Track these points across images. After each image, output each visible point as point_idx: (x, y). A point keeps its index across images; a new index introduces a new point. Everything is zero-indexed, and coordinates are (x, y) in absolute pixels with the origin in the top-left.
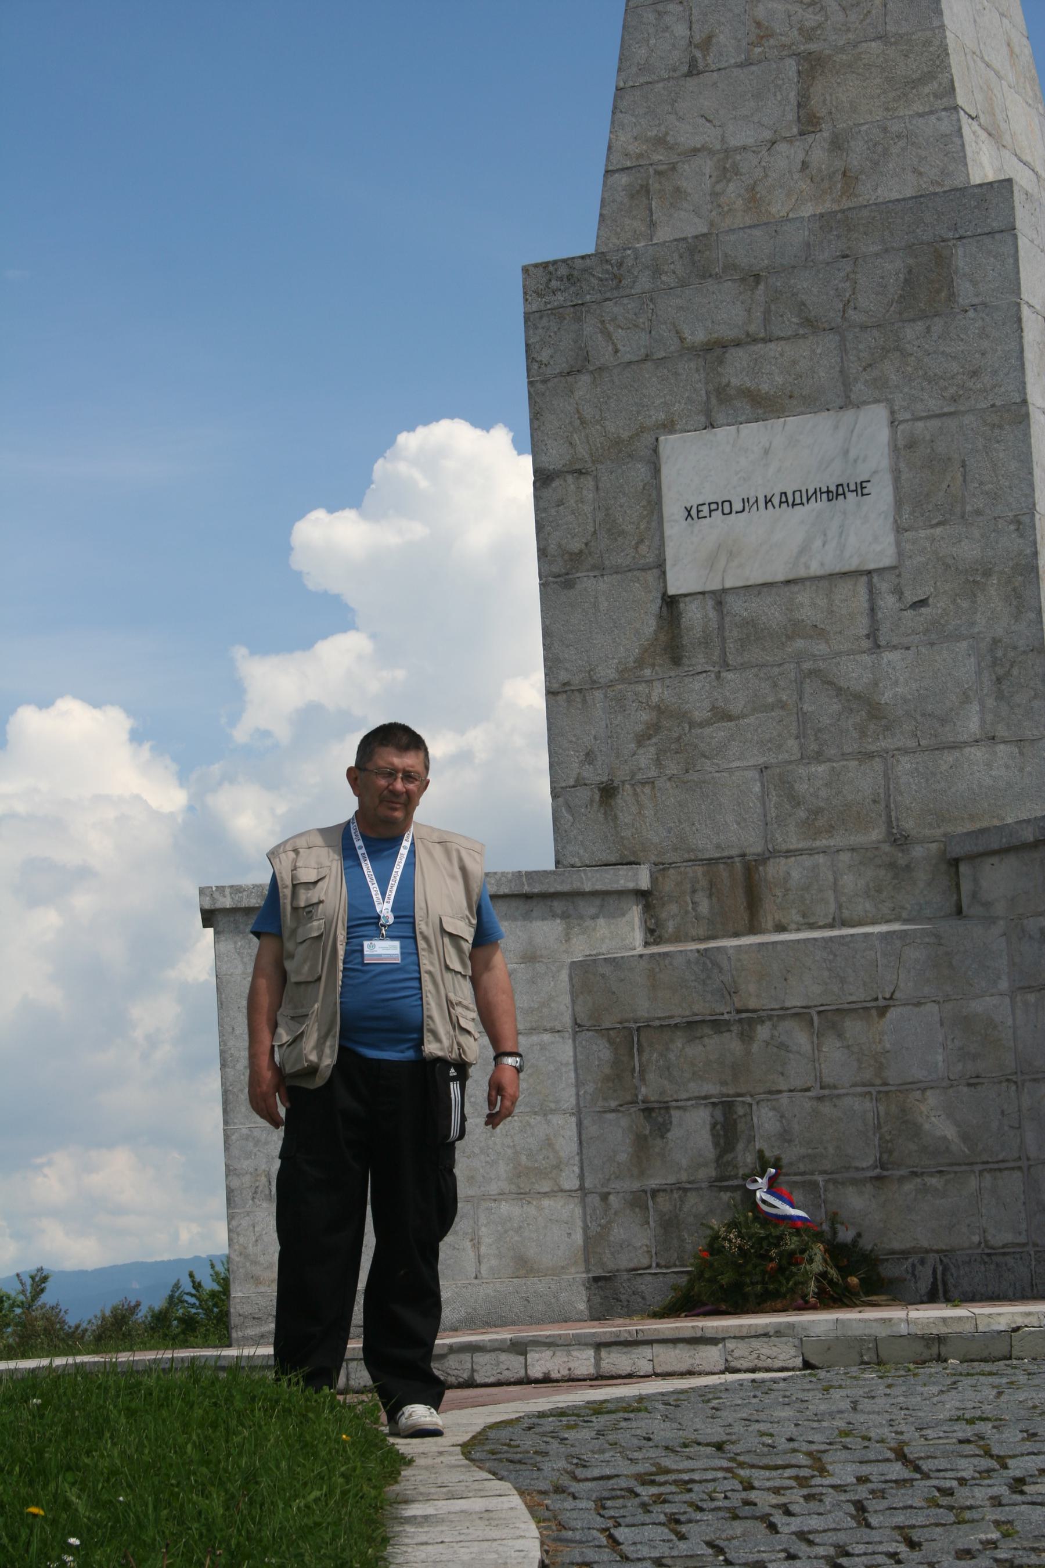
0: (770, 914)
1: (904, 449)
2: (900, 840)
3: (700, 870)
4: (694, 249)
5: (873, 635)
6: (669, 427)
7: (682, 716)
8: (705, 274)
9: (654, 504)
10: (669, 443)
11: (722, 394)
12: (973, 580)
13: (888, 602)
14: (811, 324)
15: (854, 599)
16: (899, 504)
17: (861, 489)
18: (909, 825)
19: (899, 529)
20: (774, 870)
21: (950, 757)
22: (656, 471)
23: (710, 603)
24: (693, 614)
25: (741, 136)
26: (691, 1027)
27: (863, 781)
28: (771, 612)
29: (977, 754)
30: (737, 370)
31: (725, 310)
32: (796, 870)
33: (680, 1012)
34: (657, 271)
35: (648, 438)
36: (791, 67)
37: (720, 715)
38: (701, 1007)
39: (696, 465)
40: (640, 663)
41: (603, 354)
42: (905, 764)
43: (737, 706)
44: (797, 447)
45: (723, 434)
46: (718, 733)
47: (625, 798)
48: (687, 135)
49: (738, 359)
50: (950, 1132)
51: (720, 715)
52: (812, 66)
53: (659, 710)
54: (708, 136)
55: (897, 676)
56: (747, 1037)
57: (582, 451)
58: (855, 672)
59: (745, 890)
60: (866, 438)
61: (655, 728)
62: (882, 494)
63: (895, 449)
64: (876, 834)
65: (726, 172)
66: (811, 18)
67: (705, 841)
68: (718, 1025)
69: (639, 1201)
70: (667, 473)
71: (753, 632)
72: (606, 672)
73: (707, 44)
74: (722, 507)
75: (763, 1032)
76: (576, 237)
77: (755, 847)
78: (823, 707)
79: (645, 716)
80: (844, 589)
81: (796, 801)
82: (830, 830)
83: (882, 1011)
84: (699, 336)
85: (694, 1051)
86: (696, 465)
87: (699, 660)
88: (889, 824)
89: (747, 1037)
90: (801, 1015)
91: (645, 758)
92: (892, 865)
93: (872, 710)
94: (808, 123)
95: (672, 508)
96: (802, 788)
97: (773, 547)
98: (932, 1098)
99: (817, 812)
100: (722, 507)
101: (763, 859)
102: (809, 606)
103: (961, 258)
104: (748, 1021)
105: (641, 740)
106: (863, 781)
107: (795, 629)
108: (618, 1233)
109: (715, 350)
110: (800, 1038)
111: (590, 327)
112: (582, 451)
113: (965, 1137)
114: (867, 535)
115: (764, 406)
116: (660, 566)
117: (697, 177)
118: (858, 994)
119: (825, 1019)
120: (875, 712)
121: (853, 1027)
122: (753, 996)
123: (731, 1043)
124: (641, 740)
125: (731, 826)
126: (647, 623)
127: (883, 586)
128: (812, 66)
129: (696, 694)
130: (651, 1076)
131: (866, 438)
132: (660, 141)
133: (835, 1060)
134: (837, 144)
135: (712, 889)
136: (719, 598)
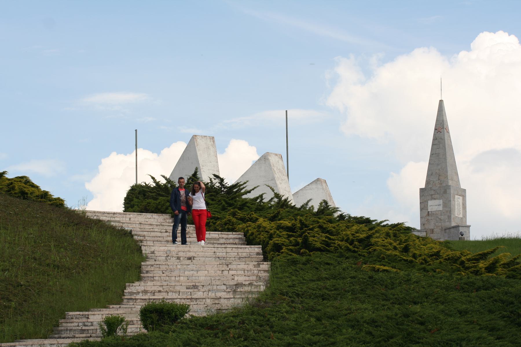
1: (443, 202)
4: (431, 188)
9: (427, 205)
12: (447, 212)
15: (440, 212)
27: (440, 224)
28: (435, 213)
30: (433, 196)
31: (433, 192)
39: (430, 203)
44: (437, 202)
48: (431, 179)
52: (439, 175)
58: (440, 217)
59: (432, 231)
60: (441, 202)
65: (433, 182)
71: (433, 214)
76: (423, 186)
78: (438, 219)
86: (430, 203)
94: (439, 179)
97: (435, 208)
102: (437, 212)
103: (447, 190)
106: (440, 224)
109: (432, 195)
114: (441, 208)
115: (435, 199)
125: (431, 227)
128: (439, 175)
129: (430, 218)
131: (441, 202)
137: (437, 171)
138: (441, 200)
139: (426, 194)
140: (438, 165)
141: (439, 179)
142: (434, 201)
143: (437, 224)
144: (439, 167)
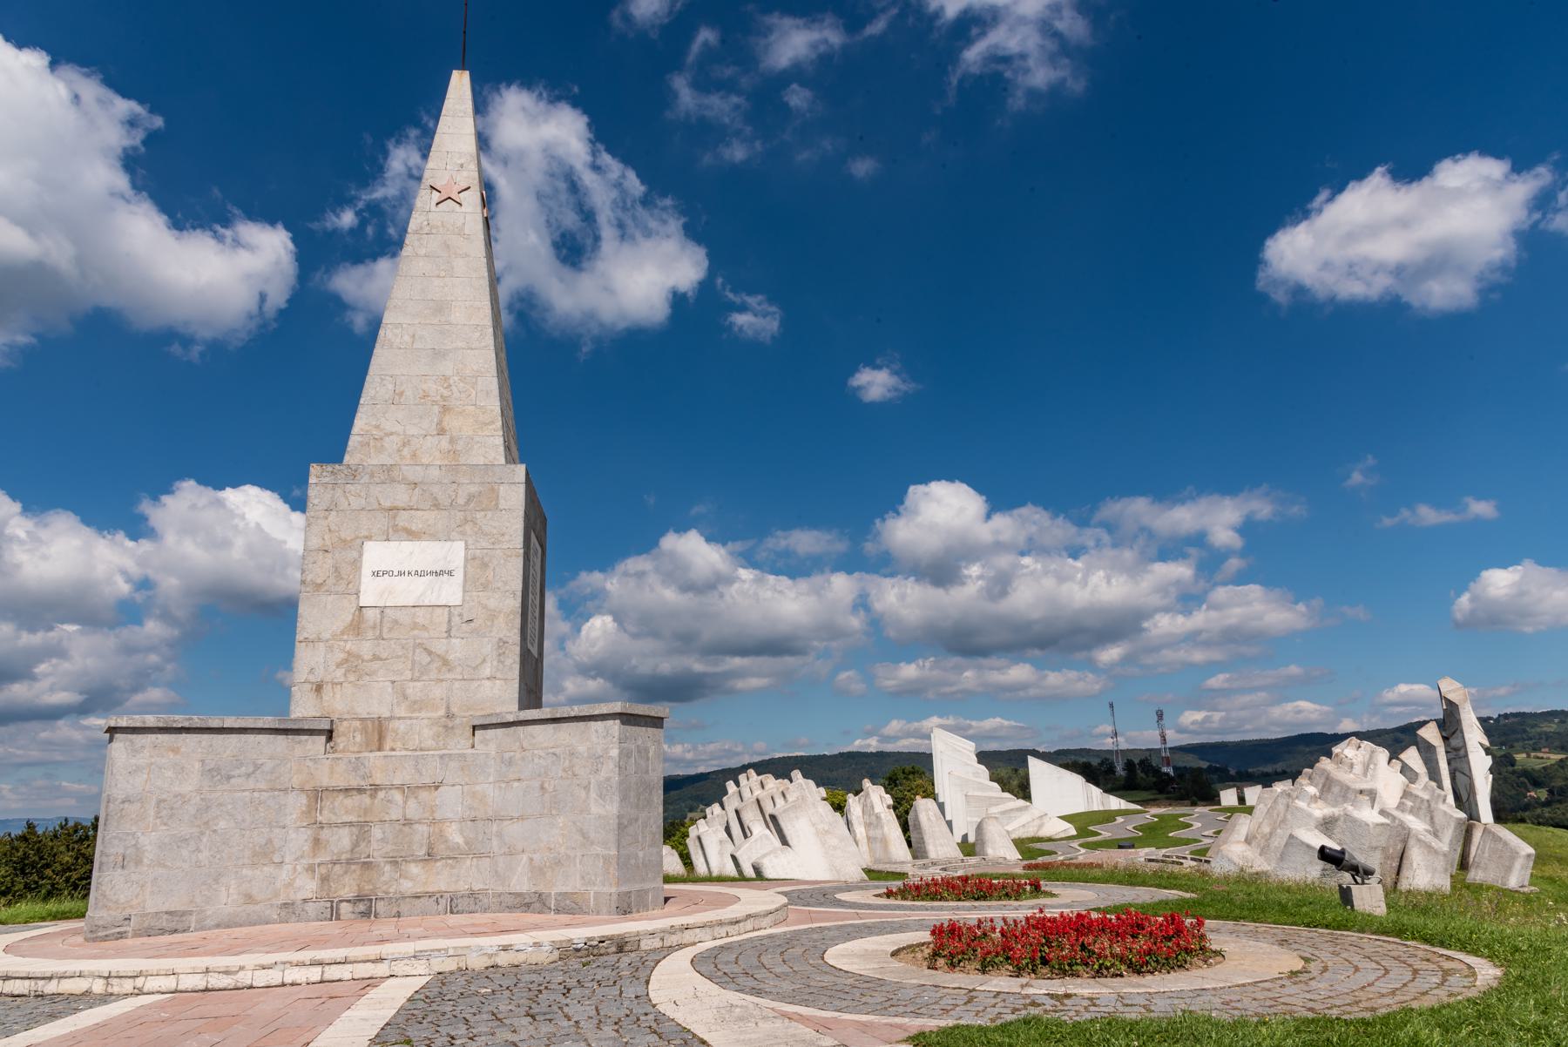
0: (388, 744)
2: (450, 716)
3: (358, 724)
5: (448, 631)
6: (369, 538)
7: (358, 657)
8: (393, 481)
10: (368, 545)
11: (396, 528)
13: (456, 620)
14: (436, 506)
16: (465, 581)
17: (450, 573)
18: (454, 710)
19: (465, 591)
20: (394, 724)
21: (476, 684)
22: (361, 555)
23: (378, 611)
24: (371, 615)
25: (413, 431)
26: (347, 791)
27: (438, 692)
28: (403, 617)
29: (487, 683)
30: (403, 519)
31: (401, 495)
32: (401, 726)
33: (343, 784)
34: (372, 476)
35: (359, 541)
36: (436, 409)
37: (376, 658)
38: (354, 783)
39: (376, 554)
40: (343, 633)
41: (343, 504)
42: (457, 685)
43: (384, 655)
45: (392, 544)
46: (376, 665)
47: (327, 689)
48: (388, 426)
49: (403, 515)
50: (459, 840)
51: (376, 658)
52: (445, 409)
53: (348, 653)
54: (399, 428)
55: (457, 649)
56: (373, 796)
57: (328, 542)
58: (439, 647)
60: (454, 553)
61: (347, 661)
62: (459, 576)
63: (466, 560)
64: (442, 712)
66: (446, 393)
68: (360, 790)
69: (311, 869)
70: (366, 557)
73: (402, 394)
75: (381, 794)
79: (343, 656)
80: (439, 611)
81: (405, 697)
82: (420, 710)
83: (437, 788)
84: (387, 504)
85: (349, 802)
86: (376, 554)
87: (370, 634)
88: (448, 708)
89: (373, 796)
90: (400, 788)
91: (339, 673)
92: (445, 726)
95: (366, 570)
96: (409, 691)
97: (409, 592)
98: (454, 826)
99: (415, 702)
101: (391, 718)
104: (376, 788)
105: (338, 666)
106: (438, 692)
107: (415, 626)
108: (298, 883)
110: (398, 797)
111: (339, 492)
112: (328, 542)
113: (467, 843)
114: (450, 592)
115: (412, 535)
116: (357, 594)
117: (391, 443)
119: (408, 790)
120: (445, 662)
121: (424, 795)
122: (379, 779)
123: (366, 799)
124: (338, 666)
126: (347, 617)
127: (456, 612)
128: (445, 409)
129: (366, 648)
130: (325, 812)
131: (454, 553)
132: (377, 427)
133: (413, 809)
134: (452, 441)
135: (364, 730)
136: (383, 609)
137: (432, 387)
138: (460, 545)
139: (356, 503)
140: (438, 354)
141: (442, 432)
142: (407, 546)
143: (414, 690)
144: (447, 367)
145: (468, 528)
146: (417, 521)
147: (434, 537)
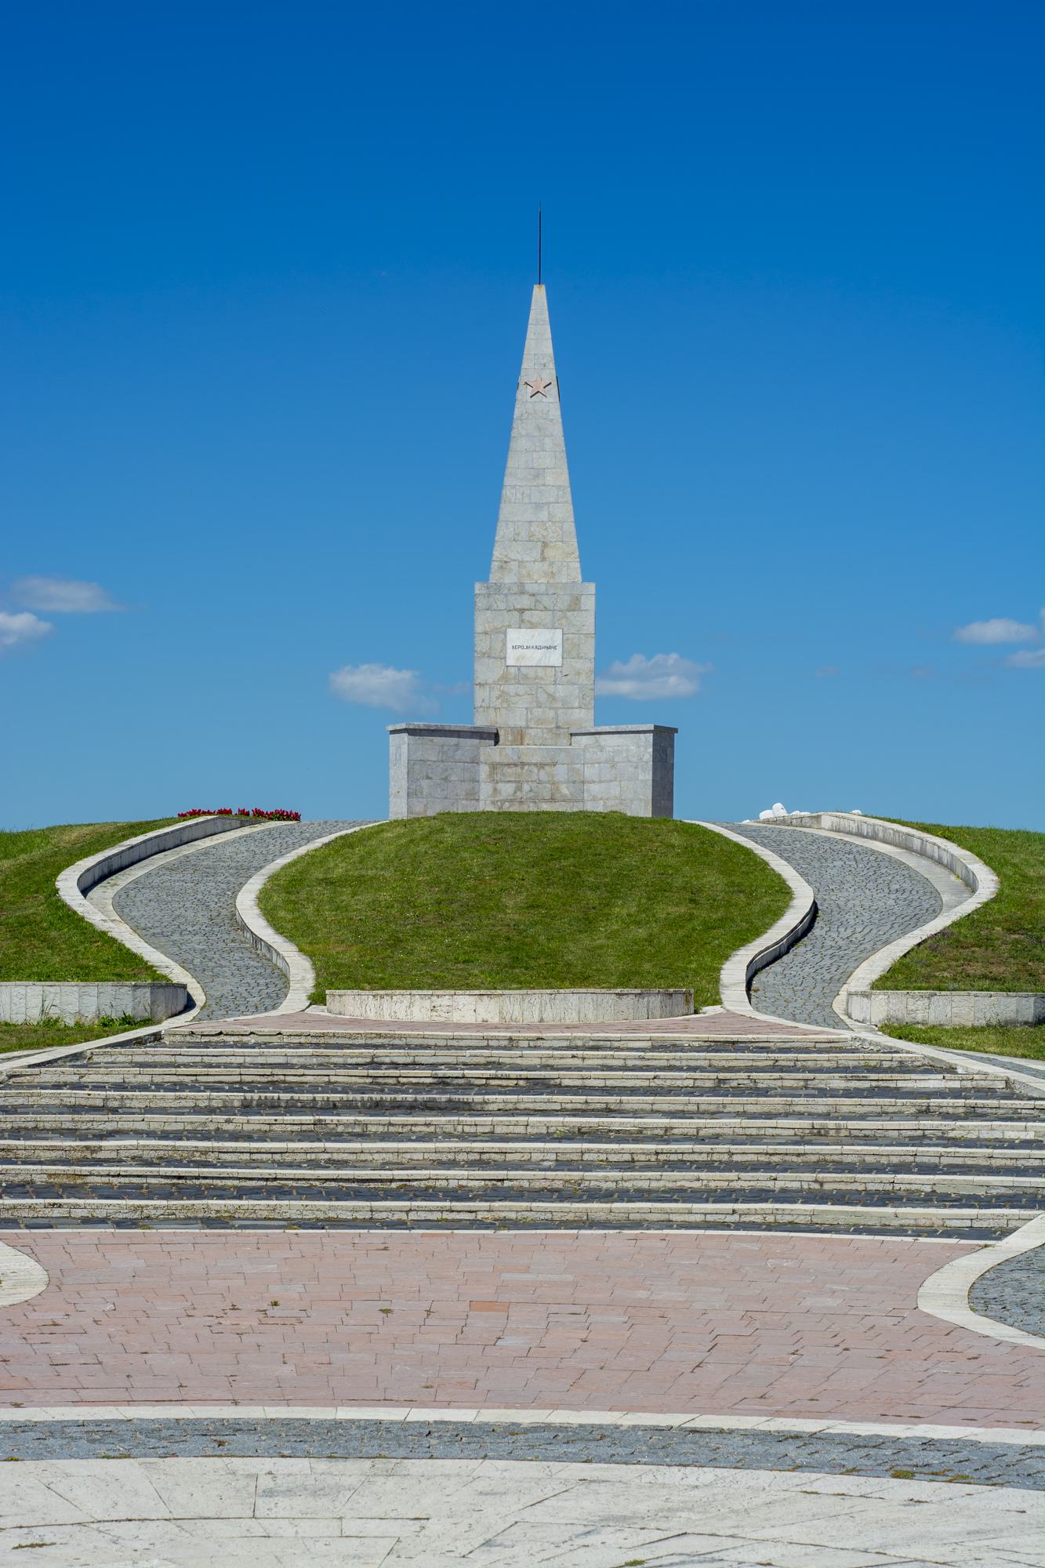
0: (526, 741)
6: (509, 626)
28: (531, 673)
30: (527, 615)
31: (525, 602)
32: (532, 732)
33: (506, 761)
37: (517, 695)
39: (515, 636)
44: (542, 636)
46: (516, 699)
51: (517, 695)
52: (545, 545)
54: (519, 557)
55: (561, 691)
58: (551, 689)
60: (557, 636)
62: (559, 649)
67: (512, 723)
71: (526, 677)
72: (490, 681)
74: (521, 647)
77: (523, 724)
84: (518, 607)
86: (515, 636)
93: (552, 697)
95: (509, 645)
97: (534, 657)
100: (521, 647)
104: (523, 764)
109: (522, 611)
110: (535, 770)
114: (555, 658)
115: (533, 626)
117: (514, 565)
118: (548, 761)
119: (541, 766)
122: (525, 759)
123: (519, 769)
128: (545, 545)
131: (557, 636)
134: (552, 564)
141: (544, 559)
144: (543, 516)
145: (563, 621)
146: (535, 616)
147: (545, 627)
